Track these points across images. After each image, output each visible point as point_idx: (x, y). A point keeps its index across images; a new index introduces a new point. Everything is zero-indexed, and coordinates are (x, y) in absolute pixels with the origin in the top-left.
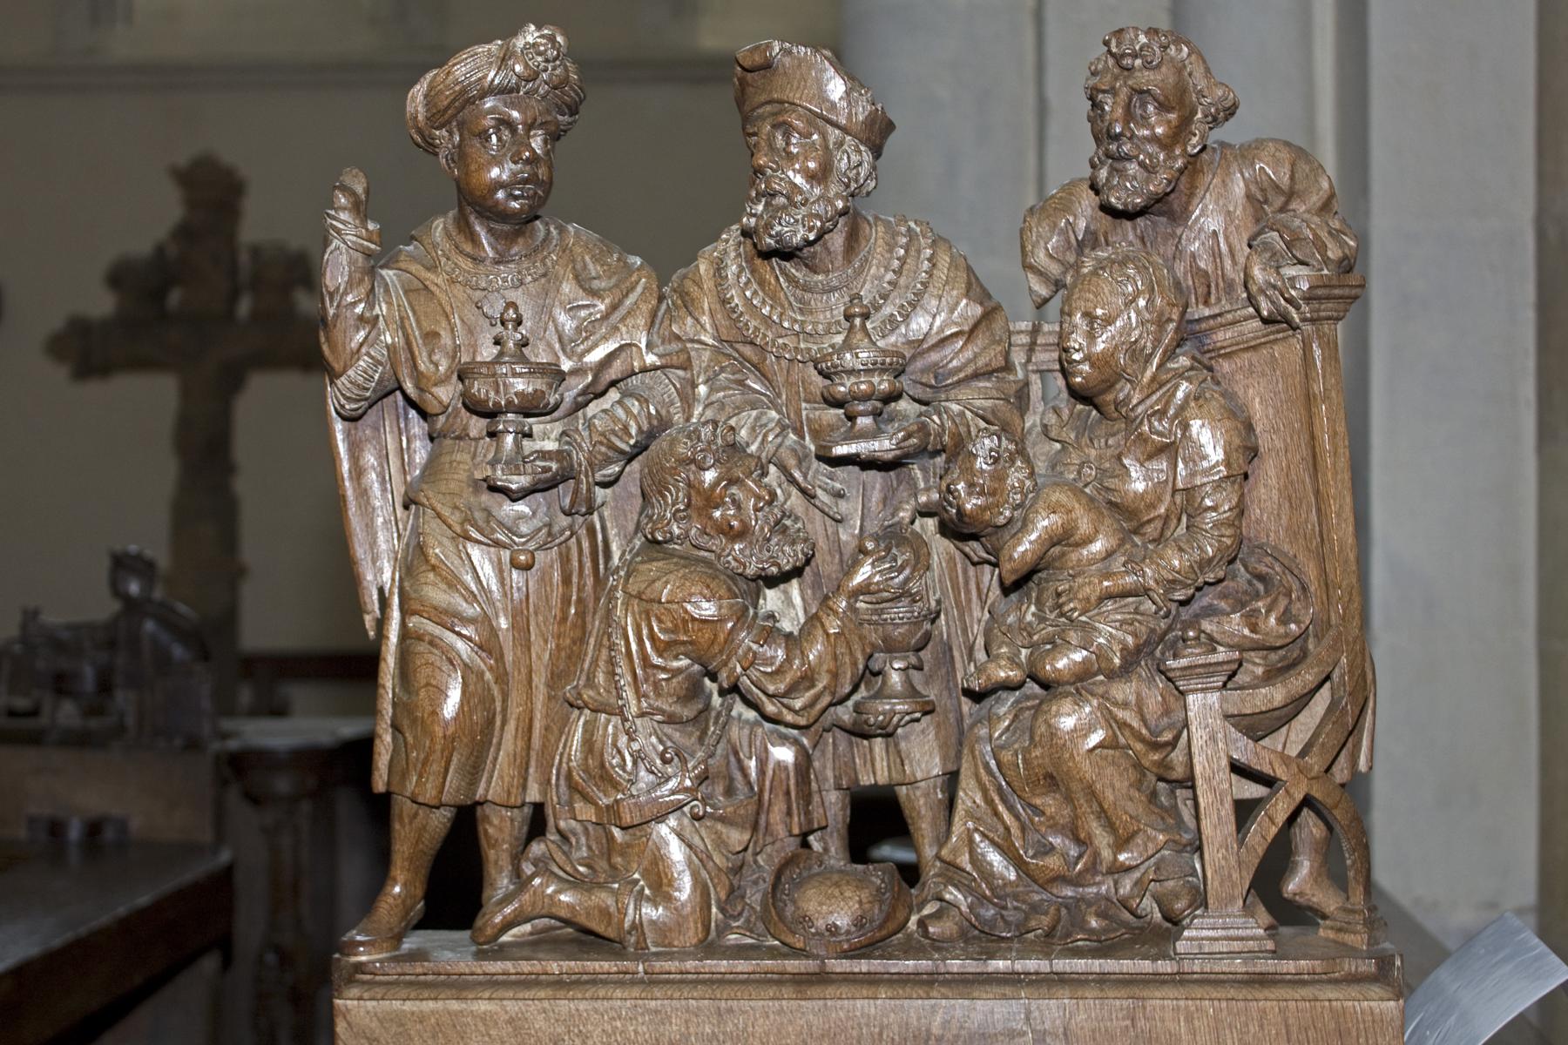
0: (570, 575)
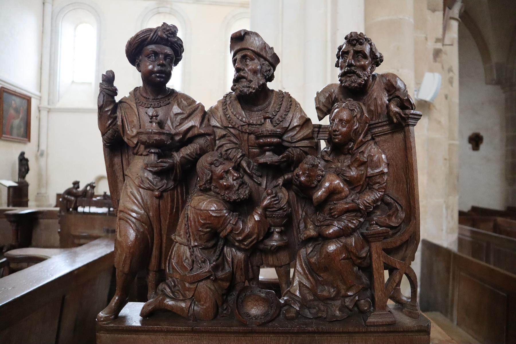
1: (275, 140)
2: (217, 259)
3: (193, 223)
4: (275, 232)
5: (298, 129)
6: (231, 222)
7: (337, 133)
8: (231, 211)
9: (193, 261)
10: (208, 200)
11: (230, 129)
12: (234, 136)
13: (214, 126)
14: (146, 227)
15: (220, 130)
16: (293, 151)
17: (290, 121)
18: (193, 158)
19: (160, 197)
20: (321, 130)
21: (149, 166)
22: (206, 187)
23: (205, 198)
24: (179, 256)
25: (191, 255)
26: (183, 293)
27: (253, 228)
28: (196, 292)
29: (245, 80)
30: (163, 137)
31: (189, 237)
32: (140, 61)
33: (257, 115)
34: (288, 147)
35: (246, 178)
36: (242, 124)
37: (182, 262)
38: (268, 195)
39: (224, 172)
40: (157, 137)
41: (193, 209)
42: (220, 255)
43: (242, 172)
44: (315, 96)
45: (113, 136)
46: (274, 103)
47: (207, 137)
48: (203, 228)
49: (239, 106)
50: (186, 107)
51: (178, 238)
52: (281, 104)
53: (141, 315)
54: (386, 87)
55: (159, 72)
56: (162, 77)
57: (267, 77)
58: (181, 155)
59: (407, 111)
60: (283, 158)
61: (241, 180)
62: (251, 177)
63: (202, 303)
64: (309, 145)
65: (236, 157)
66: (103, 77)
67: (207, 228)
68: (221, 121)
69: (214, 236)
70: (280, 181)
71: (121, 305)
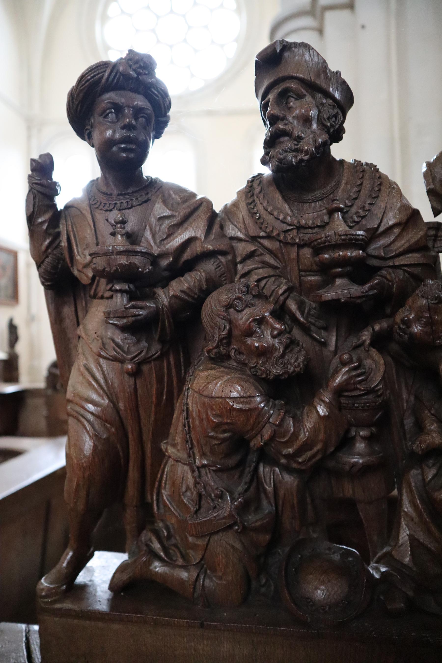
0: (163, 378)
2: (246, 490)
3: (197, 422)
4: (358, 438)
5: (396, 231)
6: (271, 420)
8: (270, 397)
9: (200, 496)
10: (225, 378)
11: (261, 241)
12: (271, 252)
13: (232, 238)
14: (113, 430)
15: (243, 244)
16: (390, 274)
17: (380, 215)
18: (193, 298)
19: (136, 374)
21: (112, 315)
22: (219, 353)
23: (219, 374)
24: (173, 484)
25: (196, 483)
26: (183, 551)
27: (315, 430)
28: (208, 551)
29: (286, 138)
31: (191, 448)
32: (92, 127)
33: (314, 208)
34: (380, 268)
35: (297, 333)
36: (286, 227)
37: (180, 496)
38: (344, 364)
39: (254, 320)
40: (123, 260)
41: (196, 395)
43: (289, 322)
44: (424, 169)
45: (54, 267)
46: (346, 184)
47: (220, 257)
48: (216, 432)
49: (278, 196)
50: (178, 204)
51: (171, 450)
52: (361, 184)
53: (111, 588)
56: (131, 151)
57: (332, 130)
58: (171, 293)
60: (371, 288)
61: (287, 335)
62: (305, 329)
63: (220, 574)
64: (423, 261)
65: (278, 291)
66: (31, 164)
67: (225, 432)
68: (246, 228)
70: (366, 336)
71: (81, 561)
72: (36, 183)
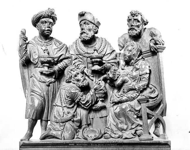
1: (98, 60)
4: (99, 101)
7: (126, 56)
20: (120, 55)
30: (50, 59)
34: (105, 63)
38: (96, 84)
42: (75, 111)
45: (26, 59)
54: (150, 34)
55: (47, 30)
56: (49, 33)
59: (157, 46)
62: (89, 77)
69: (73, 101)
72: (23, 38)
